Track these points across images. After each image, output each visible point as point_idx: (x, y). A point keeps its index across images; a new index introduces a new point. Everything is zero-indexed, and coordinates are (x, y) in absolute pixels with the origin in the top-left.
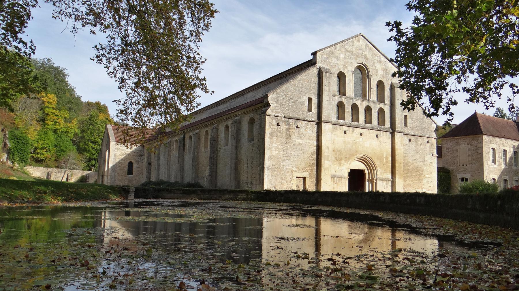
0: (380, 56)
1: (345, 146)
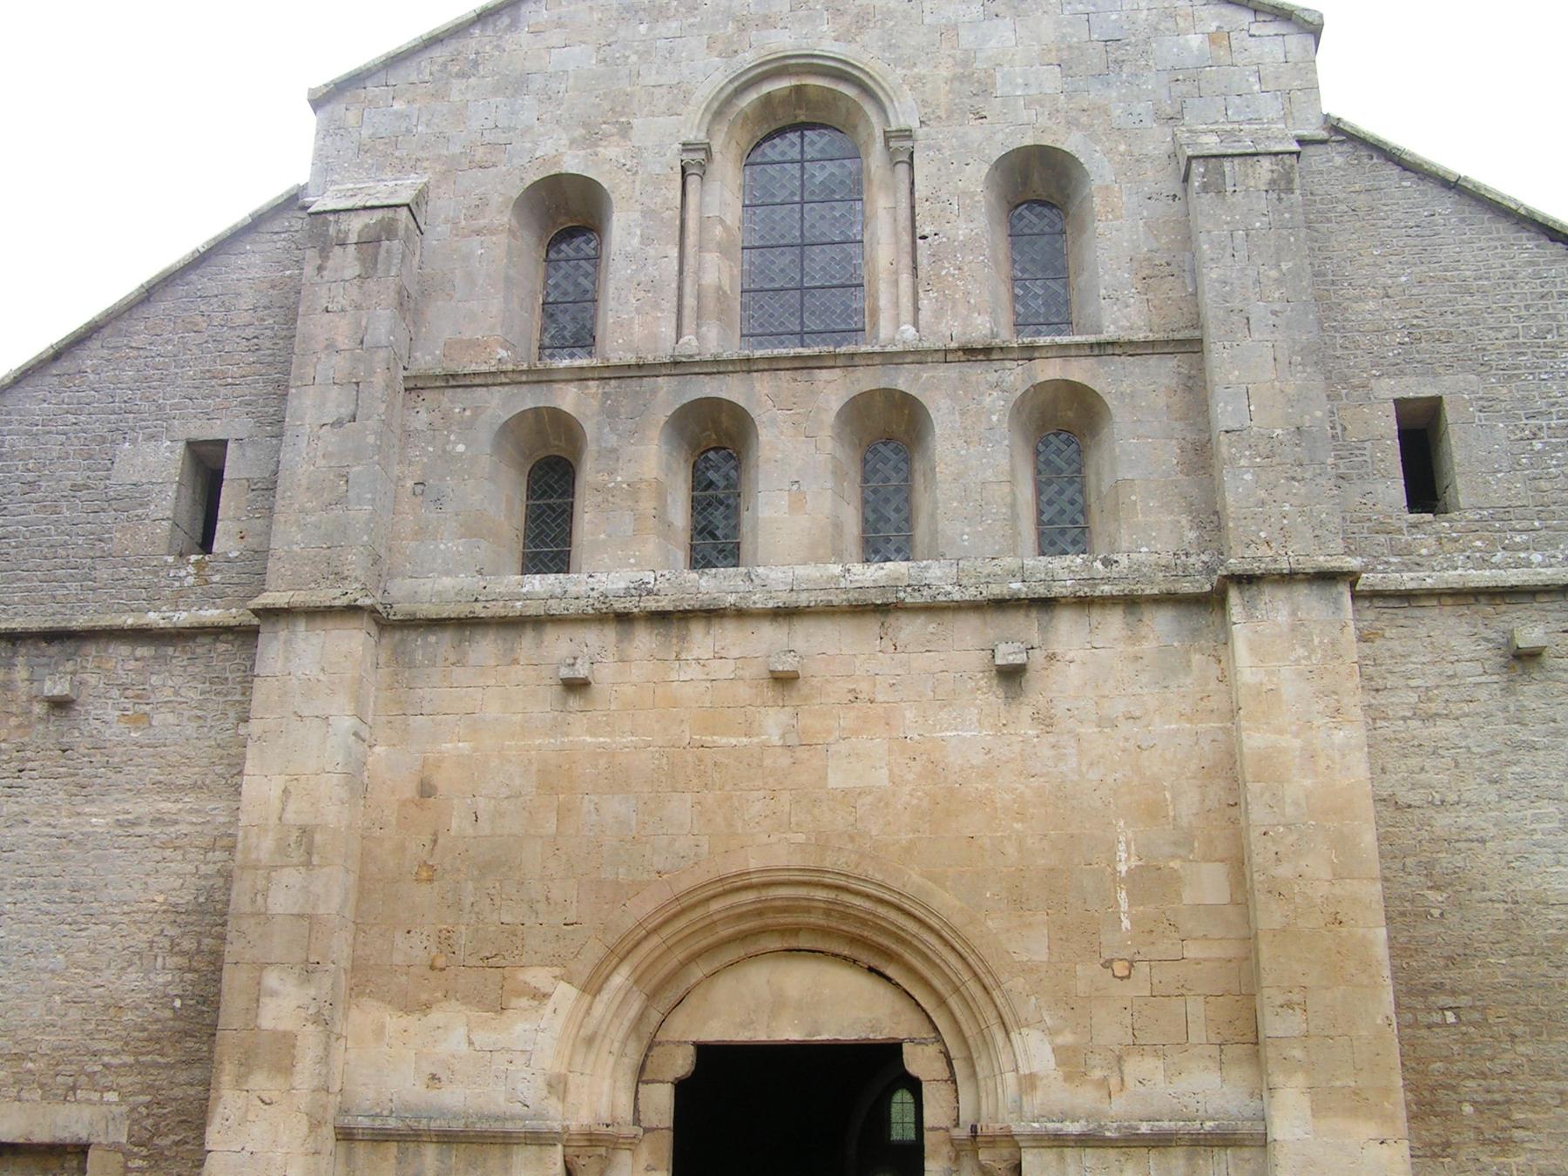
1: (563, 813)
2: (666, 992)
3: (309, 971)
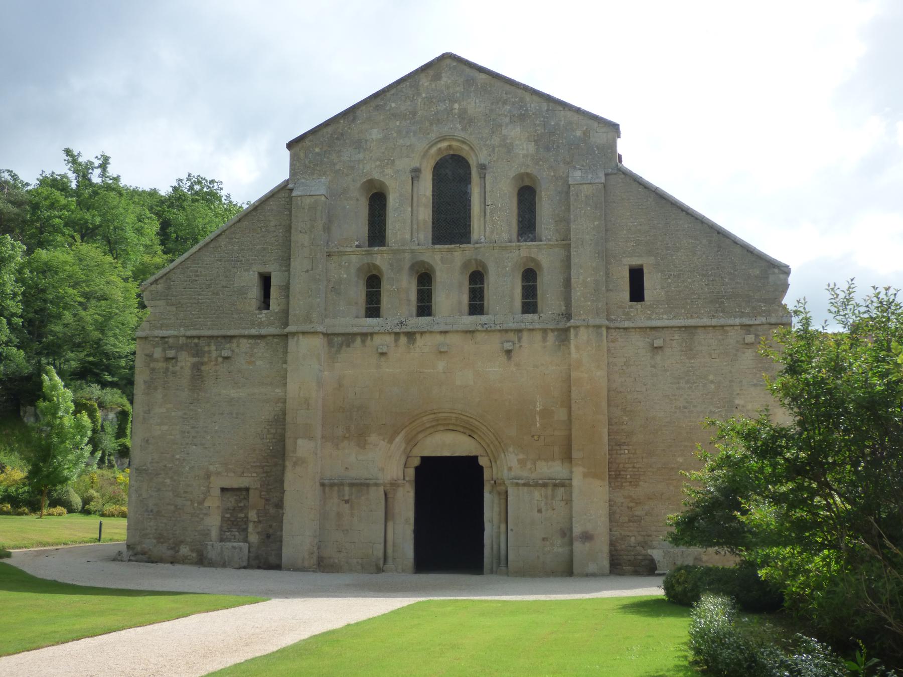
0: (522, 100)
2: (411, 442)
3: (311, 438)
